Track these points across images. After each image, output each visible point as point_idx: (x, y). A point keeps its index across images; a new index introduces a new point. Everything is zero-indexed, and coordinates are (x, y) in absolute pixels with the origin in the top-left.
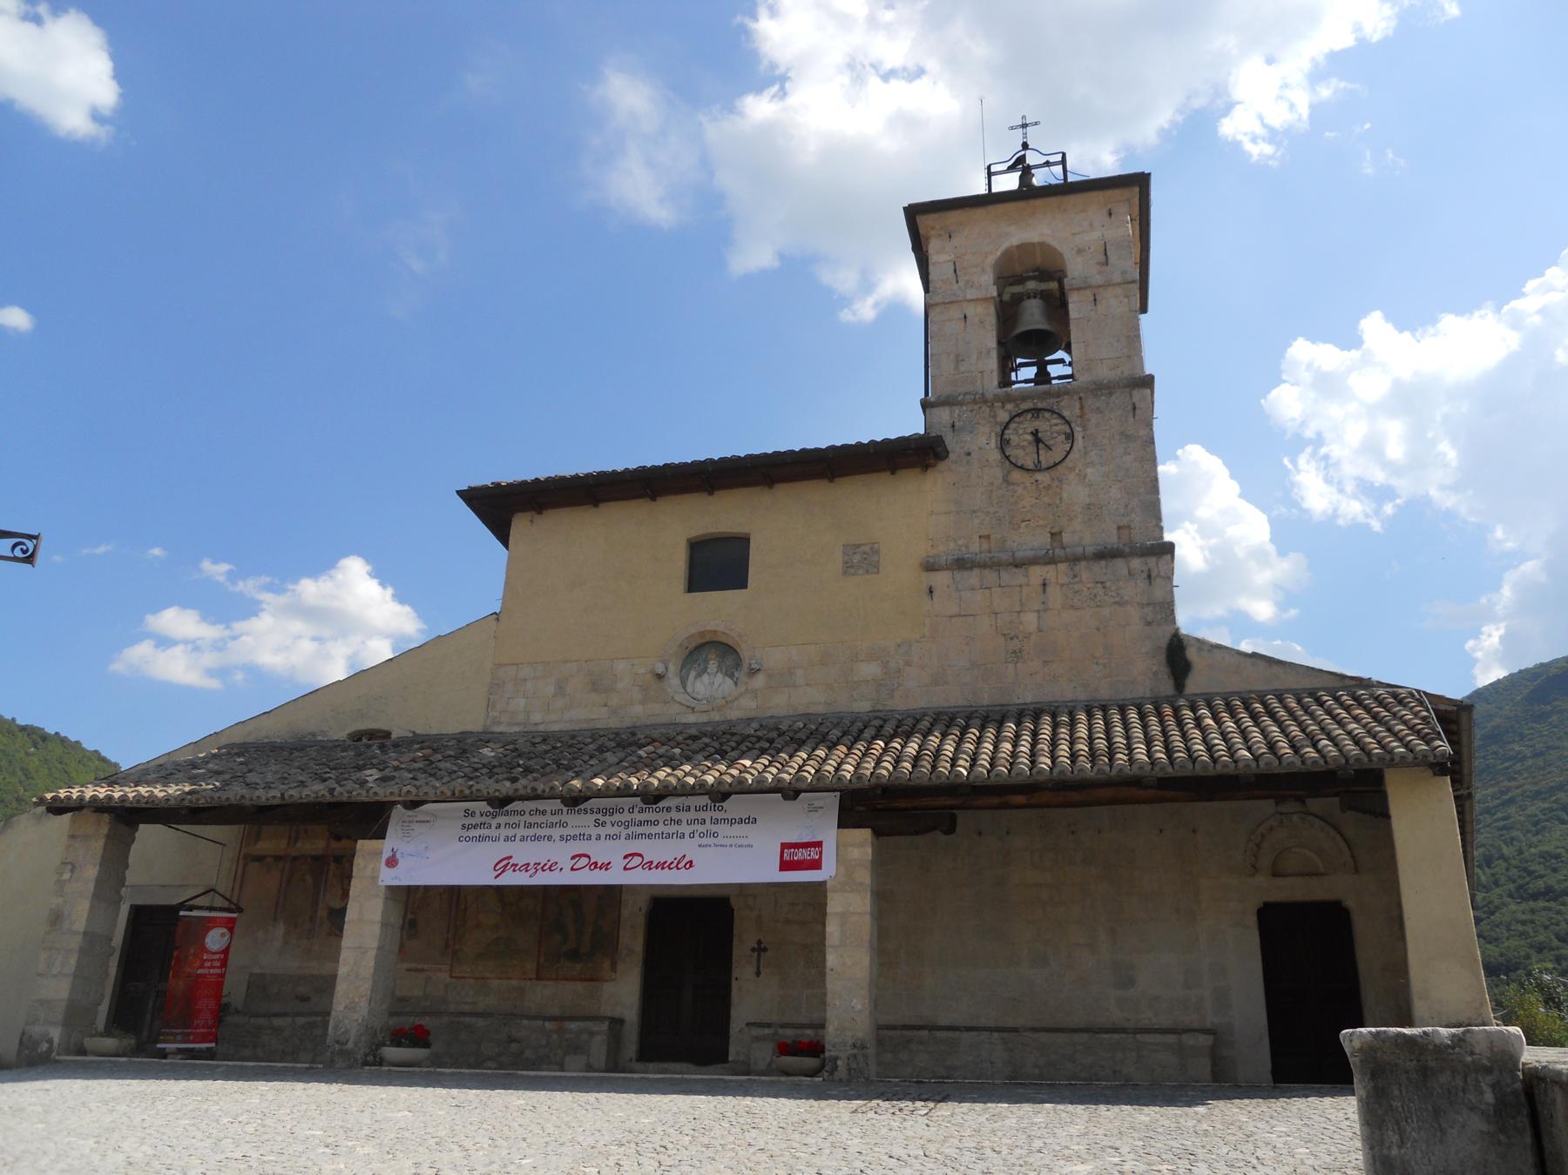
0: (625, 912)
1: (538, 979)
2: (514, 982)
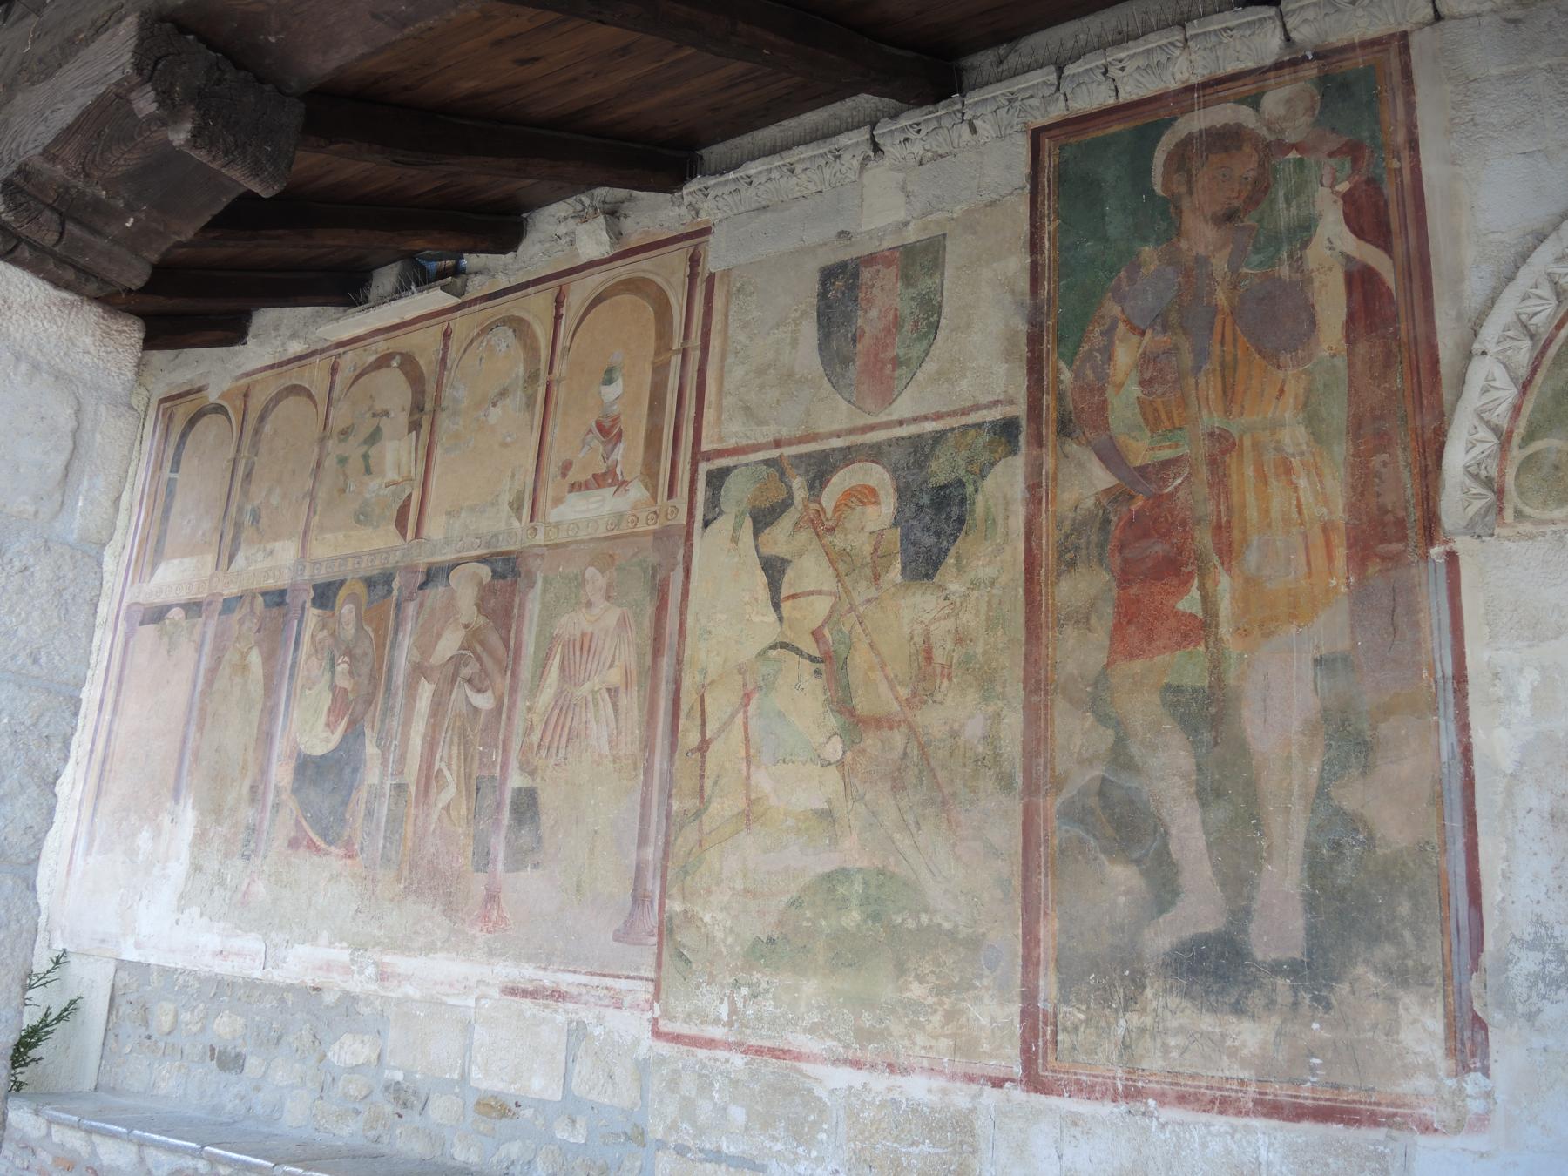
0: (1498, 741)
1: (1034, 1082)
2: (918, 1088)
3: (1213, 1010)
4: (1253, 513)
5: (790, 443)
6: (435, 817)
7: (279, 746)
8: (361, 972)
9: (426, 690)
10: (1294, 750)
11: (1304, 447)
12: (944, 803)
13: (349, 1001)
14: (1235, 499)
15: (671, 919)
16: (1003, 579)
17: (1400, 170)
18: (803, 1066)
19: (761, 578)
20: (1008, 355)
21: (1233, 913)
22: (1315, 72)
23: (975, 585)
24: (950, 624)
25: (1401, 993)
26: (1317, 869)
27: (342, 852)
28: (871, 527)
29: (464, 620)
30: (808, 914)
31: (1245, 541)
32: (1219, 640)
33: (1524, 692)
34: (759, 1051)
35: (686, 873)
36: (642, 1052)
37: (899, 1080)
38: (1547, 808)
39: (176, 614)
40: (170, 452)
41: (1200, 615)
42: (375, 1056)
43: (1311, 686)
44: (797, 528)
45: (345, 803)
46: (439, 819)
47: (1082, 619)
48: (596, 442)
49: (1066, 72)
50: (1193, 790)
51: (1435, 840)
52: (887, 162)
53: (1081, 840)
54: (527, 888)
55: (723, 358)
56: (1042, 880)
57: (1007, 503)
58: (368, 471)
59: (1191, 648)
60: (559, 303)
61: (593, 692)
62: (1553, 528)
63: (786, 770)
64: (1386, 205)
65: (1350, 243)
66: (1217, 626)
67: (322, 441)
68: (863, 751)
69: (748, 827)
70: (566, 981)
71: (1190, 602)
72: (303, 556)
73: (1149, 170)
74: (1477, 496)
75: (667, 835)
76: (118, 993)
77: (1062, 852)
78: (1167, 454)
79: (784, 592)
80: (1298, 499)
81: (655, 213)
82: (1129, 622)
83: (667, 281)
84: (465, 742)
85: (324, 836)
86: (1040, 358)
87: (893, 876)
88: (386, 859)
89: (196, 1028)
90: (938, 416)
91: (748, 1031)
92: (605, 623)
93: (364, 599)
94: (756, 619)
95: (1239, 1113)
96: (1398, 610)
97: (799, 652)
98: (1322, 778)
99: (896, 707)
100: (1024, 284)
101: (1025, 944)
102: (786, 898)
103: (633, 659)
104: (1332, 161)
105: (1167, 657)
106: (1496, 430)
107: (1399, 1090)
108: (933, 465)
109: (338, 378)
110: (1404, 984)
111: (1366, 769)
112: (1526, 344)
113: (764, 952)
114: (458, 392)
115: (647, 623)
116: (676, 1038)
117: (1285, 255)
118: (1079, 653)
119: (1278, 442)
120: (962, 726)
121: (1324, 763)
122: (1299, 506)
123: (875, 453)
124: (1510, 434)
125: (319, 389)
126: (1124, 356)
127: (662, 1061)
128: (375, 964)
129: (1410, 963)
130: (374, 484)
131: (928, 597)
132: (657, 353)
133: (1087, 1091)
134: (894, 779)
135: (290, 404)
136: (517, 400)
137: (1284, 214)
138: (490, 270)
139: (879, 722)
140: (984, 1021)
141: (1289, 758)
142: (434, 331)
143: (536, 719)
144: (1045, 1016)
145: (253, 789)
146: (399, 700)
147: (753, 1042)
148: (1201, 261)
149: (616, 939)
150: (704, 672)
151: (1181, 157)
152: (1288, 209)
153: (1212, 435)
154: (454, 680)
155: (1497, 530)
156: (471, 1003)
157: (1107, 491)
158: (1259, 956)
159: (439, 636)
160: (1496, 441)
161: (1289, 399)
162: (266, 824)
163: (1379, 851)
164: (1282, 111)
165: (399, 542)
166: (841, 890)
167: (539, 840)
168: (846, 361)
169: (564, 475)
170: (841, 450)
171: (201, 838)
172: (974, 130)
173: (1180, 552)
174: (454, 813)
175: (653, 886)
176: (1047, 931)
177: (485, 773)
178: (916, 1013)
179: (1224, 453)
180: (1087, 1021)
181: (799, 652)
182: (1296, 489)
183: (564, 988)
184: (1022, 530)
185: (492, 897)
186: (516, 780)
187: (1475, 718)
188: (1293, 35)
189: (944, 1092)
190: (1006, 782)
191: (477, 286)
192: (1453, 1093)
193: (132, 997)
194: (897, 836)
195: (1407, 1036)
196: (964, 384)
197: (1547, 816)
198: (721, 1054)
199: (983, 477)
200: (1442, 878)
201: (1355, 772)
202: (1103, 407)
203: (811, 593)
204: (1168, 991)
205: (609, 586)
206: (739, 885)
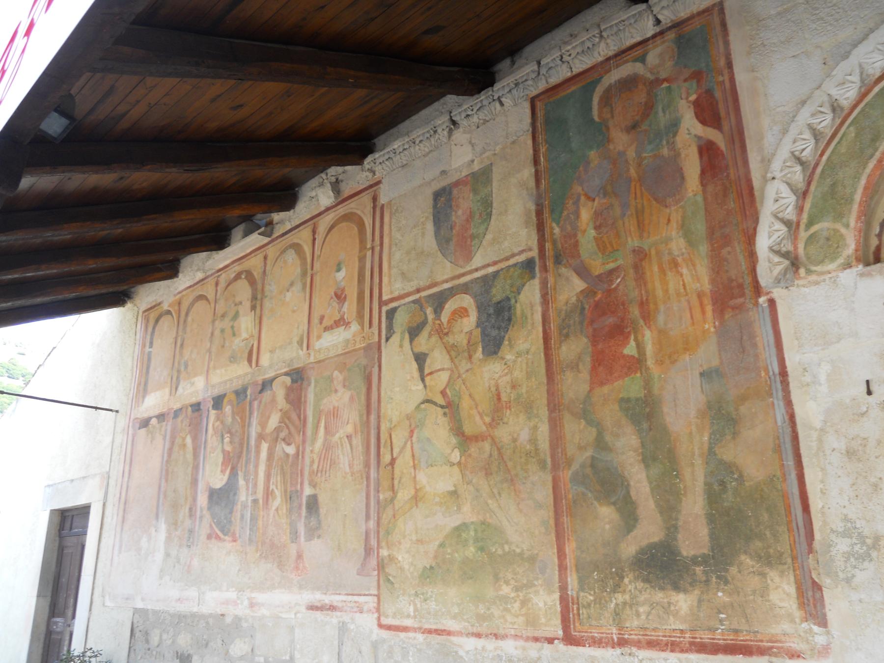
0: (810, 410)
1: (570, 639)
2: (510, 647)
3: (662, 589)
4: (659, 293)
5: (424, 289)
6: (272, 515)
7: (201, 486)
8: (242, 604)
9: (265, 446)
10: (694, 428)
11: (684, 250)
12: (512, 480)
13: (238, 619)
14: (650, 286)
15: (382, 560)
16: (533, 349)
17: (723, 81)
18: (454, 639)
19: (415, 365)
20: (527, 224)
21: (668, 529)
22: (673, 35)
23: (519, 354)
24: (508, 378)
25: (767, 570)
26: (713, 497)
27: (230, 539)
28: (466, 329)
29: (279, 408)
30: (449, 551)
31: (657, 309)
32: (647, 369)
33: (823, 378)
34: (430, 632)
35: (388, 533)
36: (374, 637)
37: (500, 643)
38: (844, 447)
39: (154, 421)
40: (148, 337)
41: (636, 356)
42: (250, 650)
43: (699, 389)
44: (430, 335)
45: (231, 512)
46: (274, 516)
47: (574, 366)
48: (335, 304)
49: (542, 63)
50: (640, 458)
51: (779, 473)
52: (461, 130)
53: (583, 494)
54: (316, 550)
55: (390, 248)
56: (565, 520)
57: (532, 306)
58: (234, 335)
59: (633, 375)
60: (314, 232)
61: (340, 438)
62: (830, 275)
63: (434, 469)
64: (717, 103)
65: (699, 129)
66: (646, 361)
67: (213, 322)
68: (470, 455)
69: (417, 506)
70: (336, 599)
71: (630, 349)
72: (207, 383)
73: (591, 109)
74: (779, 263)
75: (378, 513)
76: (135, 626)
77: (574, 502)
78: (612, 266)
79: (426, 371)
80: (683, 281)
81: (354, 176)
82: (599, 365)
83: (363, 212)
84: (283, 474)
85: (222, 531)
86: (543, 222)
87: (489, 525)
88: (250, 540)
89: (169, 642)
90: (495, 263)
91: (424, 621)
92: (343, 399)
93: (235, 403)
94: (414, 388)
95: (682, 651)
96: (745, 337)
97: (435, 404)
98: (710, 443)
99: (484, 428)
100: (532, 183)
101: (559, 557)
102: (437, 543)
103: (357, 419)
104: (686, 84)
105: (620, 382)
106: (787, 223)
107: (773, 631)
108: (494, 291)
109: (219, 288)
110: (769, 564)
111: (735, 435)
112: (798, 168)
113: (429, 574)
114: (272, 288)
115: (363, 398)
116: (389, 628)
117: (664, 142)
118: (575, 385)
119: (670, 249)
120: (518, 435)
121: (711, 434)
122: (684, 285)
123: (465, 289)
124: (798, 224)
125: (210, 294)
126: (585, 215)
127: (384, 641)
128: (248, 599)
129: (771, 551)
130: (237, 341)
131: (496, 364)
132: (360, 251)
133: (597, 643)
134: (486, 469)
135: (200, 305)
136: (298, 287)
137: (662, 119)
138: (283, 219)
139: (477, 438)
140: (541, 605)
141: (691, 433)
142: (260, 257)
143: (315, 456)
144: (573, 599)
145: (191, 509)
146: (253, 454)
147: (427, 626)
148: (622, 154)
149: (358, 574)
150: (391, 421)
151: (606, 99)
152: (664, 116)
153: (634, 251)
154: (276, 440)
155: (796, 282)
156: (293, 616)
157: (582, 292)
158: (685, 554)
159: (269, 418)
160: (786, 229)
161: (674, 224)
162: (197, 528)
163: (747, 484)
164: (657, 61)
165: (249, 370)
166: (464, 535)
167: (319, 522)
168: (448, 241)
169: (321, 323)
170: (449, 289)
171: (169, 539)
172: (502, 104)
173: (623, 320)
174: (280, 512)
175: (373, 542)
176: (570, 548)
177: (293, 489)
178: (506, 603)
179: (641, 260)
180: (595, 600)
181: (435, 404)
182: (682, 275)
183: (335, 604)
184: (540, 320)
185: (300, 556)
186: (308, 491)
187: (795, 397)
188: (660, 17)
189: (524, 649)
190: (542, 464)
191: (279, 231)
192: (806, 632)
193: (141, 628)
194: (490, 502)
195: (774, 597)
196: (506, 244)
197: (844, 452)
198: (411, 634)
199: (519, 293)
200: (785, 496)
201: (729, 437)
202: (576, 244)
203: (439, 370)
204: (636, 578)
205: (344, 380)
206: (414, 538)
